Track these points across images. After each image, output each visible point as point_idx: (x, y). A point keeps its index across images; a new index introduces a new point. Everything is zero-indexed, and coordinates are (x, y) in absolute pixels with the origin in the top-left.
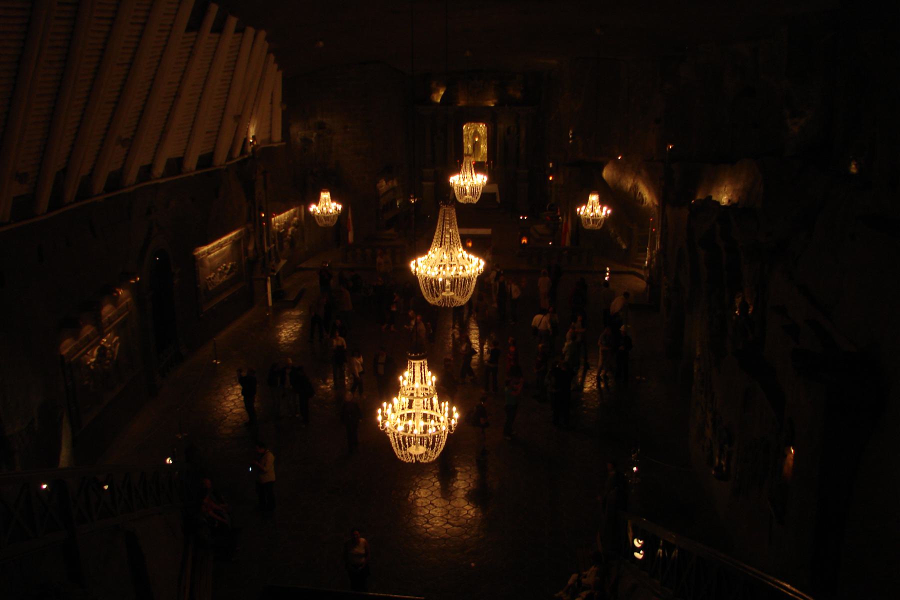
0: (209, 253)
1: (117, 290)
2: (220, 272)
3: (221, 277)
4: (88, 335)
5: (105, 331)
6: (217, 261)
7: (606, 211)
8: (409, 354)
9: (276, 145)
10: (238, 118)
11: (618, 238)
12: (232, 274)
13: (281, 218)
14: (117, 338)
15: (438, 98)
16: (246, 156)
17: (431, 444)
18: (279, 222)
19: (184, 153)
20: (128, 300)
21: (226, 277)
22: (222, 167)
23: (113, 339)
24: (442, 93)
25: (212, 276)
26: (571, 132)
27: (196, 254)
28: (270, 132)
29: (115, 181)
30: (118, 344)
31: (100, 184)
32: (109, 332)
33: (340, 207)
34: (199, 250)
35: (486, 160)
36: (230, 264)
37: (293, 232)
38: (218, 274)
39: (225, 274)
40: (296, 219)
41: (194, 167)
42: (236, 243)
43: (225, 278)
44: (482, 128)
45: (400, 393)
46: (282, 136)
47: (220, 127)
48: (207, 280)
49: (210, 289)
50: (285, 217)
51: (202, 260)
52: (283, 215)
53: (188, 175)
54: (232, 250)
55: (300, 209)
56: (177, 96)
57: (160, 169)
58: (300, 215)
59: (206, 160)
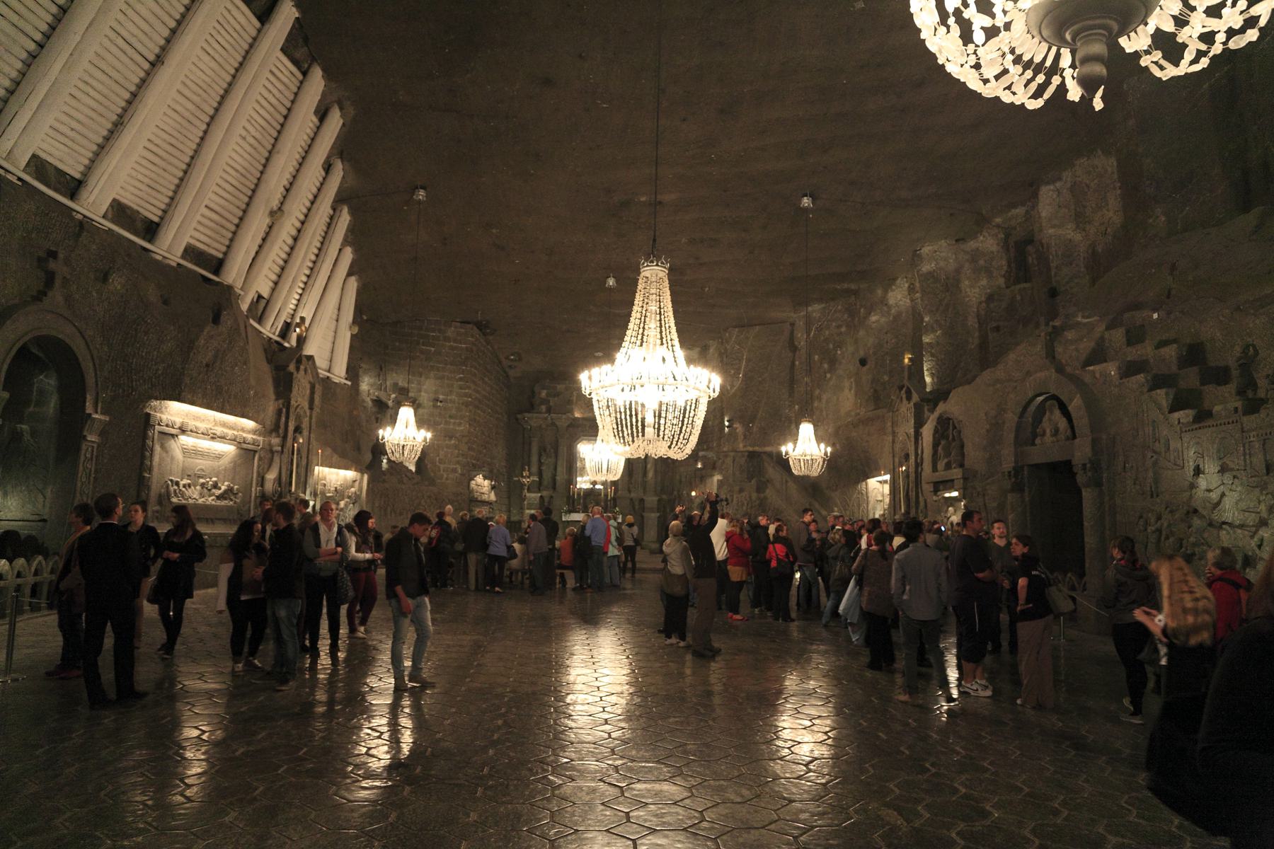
2: (203, 485)
3: (202, 495)
6: (201, 464)
7: (825, 449)
9: (336, 380)
16: (286, 345)
19: (162, 218)
21: (213, 500)
25: (185, 481)
26: (726, 419)
33: (429, 435)
39: (213, 494)
40: (353, 490)
43: (211, 500)
46: (347, 372)
48: (171, 481)
55: (362, 479)
58: (361, 489)
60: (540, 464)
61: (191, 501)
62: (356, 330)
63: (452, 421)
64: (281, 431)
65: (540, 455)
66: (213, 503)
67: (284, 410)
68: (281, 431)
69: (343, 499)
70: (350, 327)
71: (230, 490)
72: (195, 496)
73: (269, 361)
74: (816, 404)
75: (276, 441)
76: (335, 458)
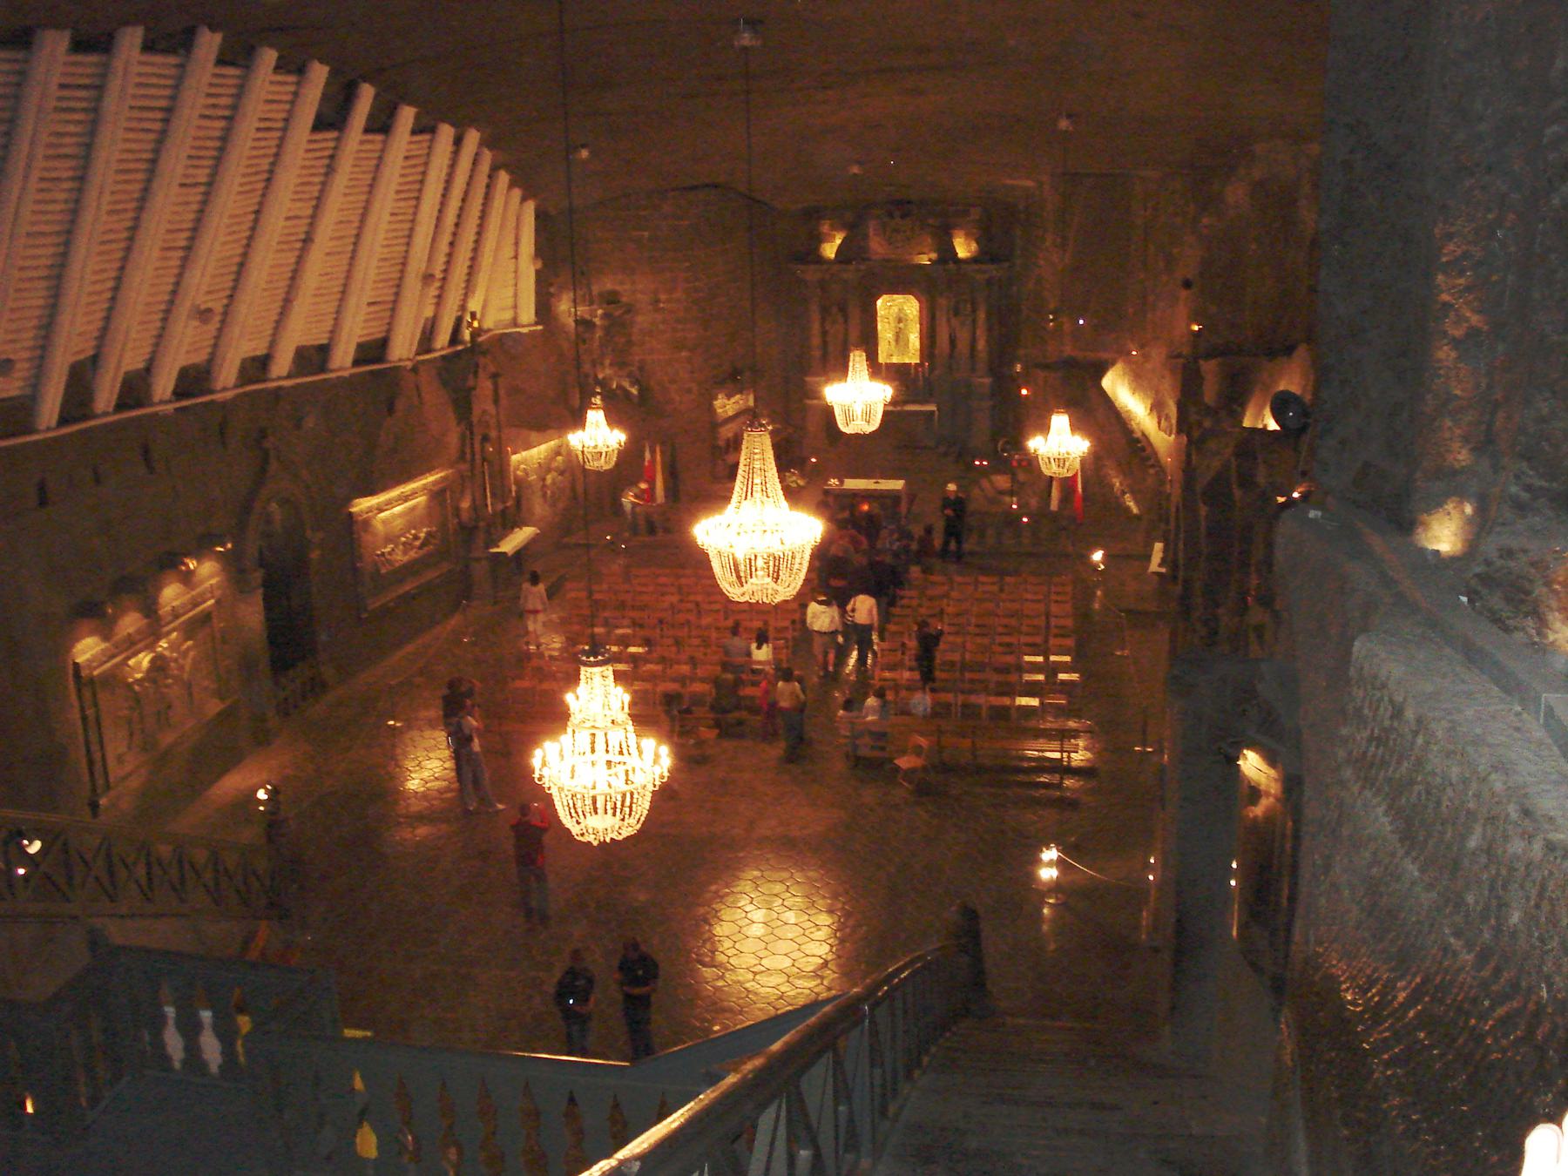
0: (381, 511)
1: (187, 561)
2: (404, 544)
3: (405, 553)
4: (129, 635)
5: (166, 629)
6: (399, 523)
8: (584, 658)
9: (525, 330)
10: (440, 281)
11: (1128, 495)
12: (426, 549)
13: (531, 456)
14: (190, 643)
15: (830, 250)
16: (460, 348)
17: (621, 807)
18: (524, 461)
19: (331, 339)
20: (213, 581)
22: (401, 364)
23: (182, 644)
24: (838, 241)
25: (388, 550)
27: (353, 510)
28: (515, 307)
29: (193, 381)
30: (192, 654)
31: (164, 384)
32: (174, 630)
34: (360, 504)
35: (915, 360)
36: (425, 530)
37: (554, 483)
38: (401, 547)
41: (349, 360)
42: (437, 495)
43: (413, 554)
44: (910, 306)
45: (569, 723)
46: (537, 313)
47: (397, 294)
48: (378, 555)
49: (383, 571)
50: (539, 453)
51: (367, 524)
52: (534, 451)
53: (339, 374)
54: (429, 507)
56: (308, 240)
57: (282, 364)
59: (373, 351)
60: (824, 333)
61: (397, 565)
62: (539, 265)
63: (680, 327)
64: (468, 456)
65: (823, 320)
66: (416, 556)
67: (468, 432)
68: (468, 456)
69: (549, 470)
70: (534, 264)
71: (429, 534)
72: (399, 558)
73: (445, 384)
74: (1149, 316)
75: (464, 467)
76: (534, 436)
